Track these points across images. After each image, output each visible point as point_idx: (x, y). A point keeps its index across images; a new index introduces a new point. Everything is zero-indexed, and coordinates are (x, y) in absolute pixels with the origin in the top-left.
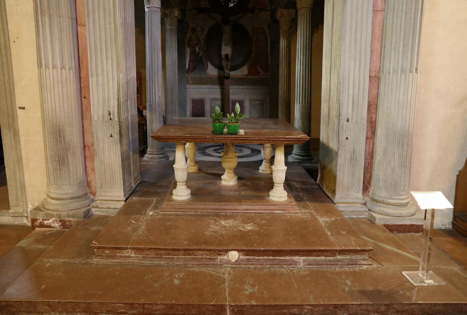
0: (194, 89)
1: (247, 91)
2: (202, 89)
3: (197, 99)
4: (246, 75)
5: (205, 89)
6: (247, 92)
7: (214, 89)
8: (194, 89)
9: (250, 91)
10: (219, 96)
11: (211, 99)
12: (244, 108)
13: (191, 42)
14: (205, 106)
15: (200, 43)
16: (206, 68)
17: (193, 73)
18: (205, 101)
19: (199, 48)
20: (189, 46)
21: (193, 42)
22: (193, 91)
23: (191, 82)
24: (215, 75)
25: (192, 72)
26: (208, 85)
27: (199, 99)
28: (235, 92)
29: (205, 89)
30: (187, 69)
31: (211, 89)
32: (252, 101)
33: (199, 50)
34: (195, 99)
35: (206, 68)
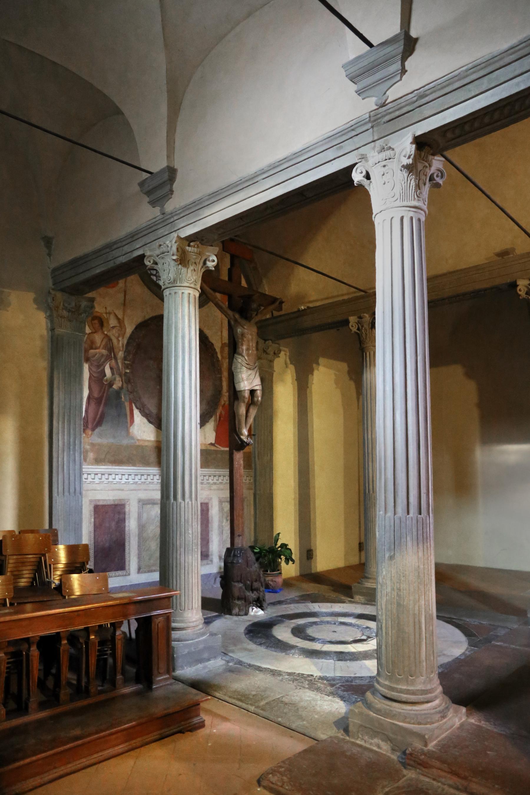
0: (99, 475)
1: (215, 481)
3: (109, 503)
5: (126, 476)
6: (215, 484)
8: (99, 475)
9: (220, 481)
10: (157, 495)
11: (140, 501)
12: (210, 521)
13: (92, 351)
14: (127, 524)
15: (114, 355)
16: (129, 421)
17: (97, 430)
18: (127, 510)
19: (111, 368)
20: (87, 360)
22: (97, 480)
23: (91, 455)
24: (148, 441)
25: (93, 430)
27: (112, 503)
29: (126, 476)
32: (223, 503)
33: (113, 374)
34: (101, 503)
35: (129, 421)
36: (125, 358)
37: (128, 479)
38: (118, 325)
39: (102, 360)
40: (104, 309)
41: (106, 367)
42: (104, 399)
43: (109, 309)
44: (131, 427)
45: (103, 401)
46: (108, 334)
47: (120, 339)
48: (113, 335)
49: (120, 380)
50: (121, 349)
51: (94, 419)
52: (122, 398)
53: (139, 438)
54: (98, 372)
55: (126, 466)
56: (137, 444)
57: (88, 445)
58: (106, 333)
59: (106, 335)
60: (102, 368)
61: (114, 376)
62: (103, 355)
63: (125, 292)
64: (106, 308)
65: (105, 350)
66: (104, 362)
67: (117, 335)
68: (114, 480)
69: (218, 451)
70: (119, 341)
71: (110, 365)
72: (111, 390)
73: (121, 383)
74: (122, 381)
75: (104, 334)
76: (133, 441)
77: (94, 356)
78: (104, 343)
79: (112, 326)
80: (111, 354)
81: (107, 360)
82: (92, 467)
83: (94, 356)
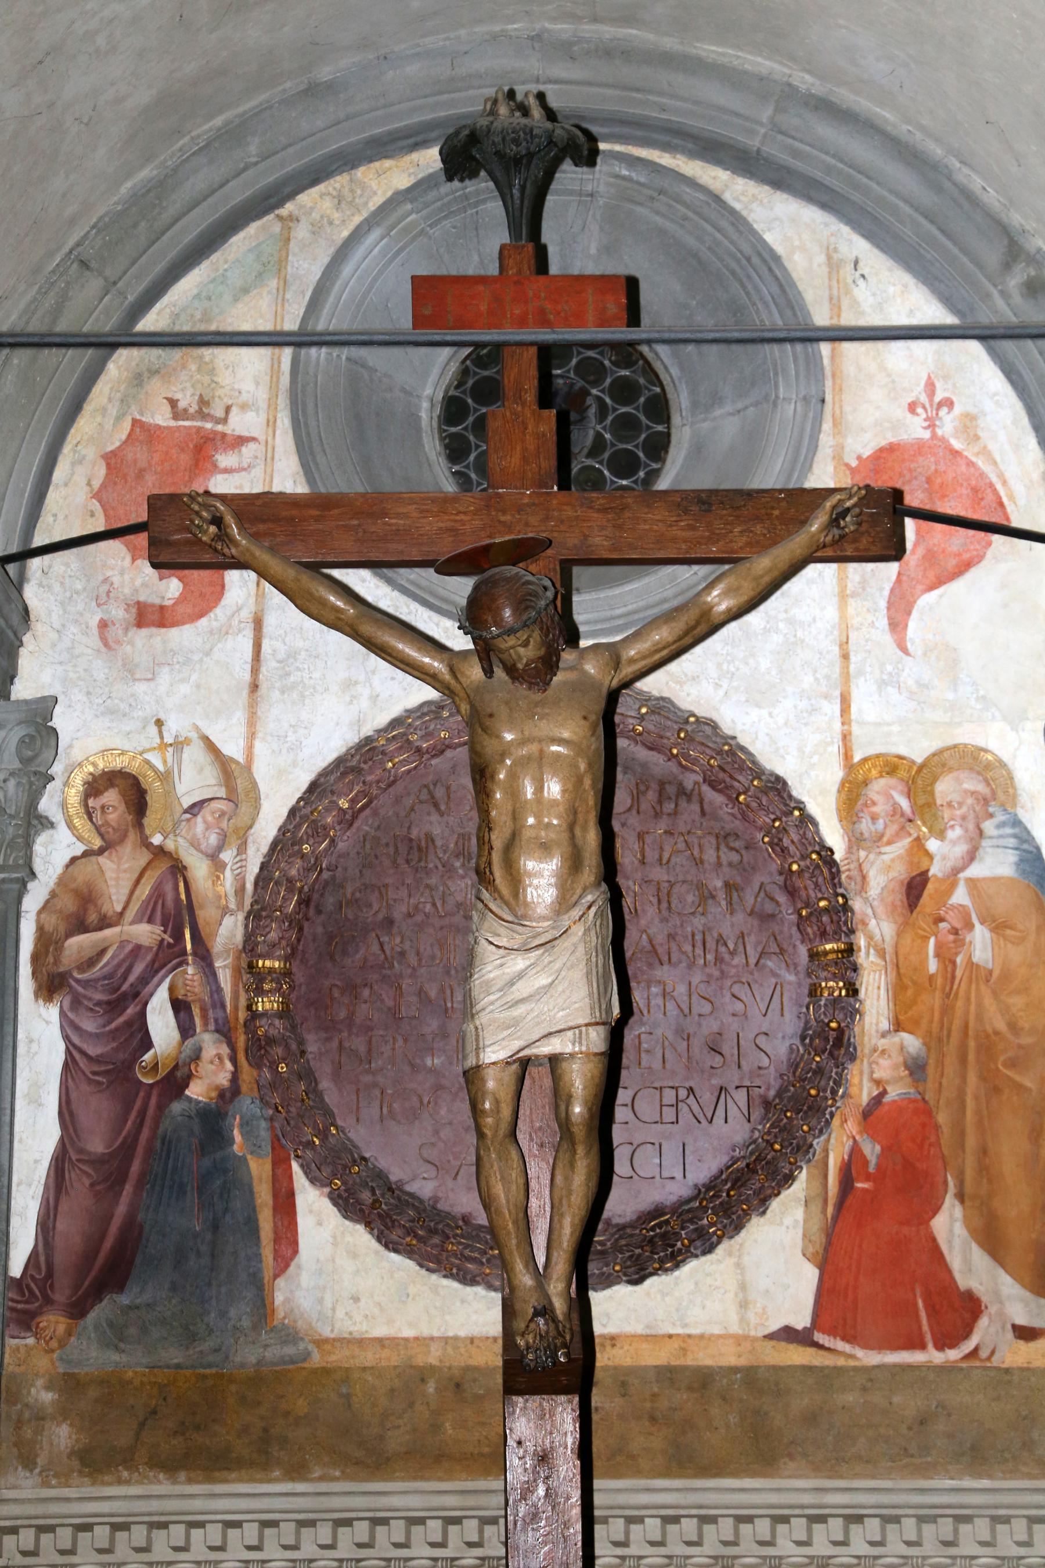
2: (214, 1535)
4: (788, 1334)
5: (251, 1533)
7: (376, 1522)
17: (100, 1312)
19: (179, 1006)
21: (107, 932)
25: (78, 1310)
26: (297, 1471)
28: (654, 1557)
30: (16, 1270)
31: (324, 1533)
33: (186, 1030)
36: (250, 947)
37: (258, 1548)
38: (222, 793)
39: (139, 969)
40: (153, 730)
41: (149, 1007)
42: (140, 1150)
43: (174, 727)
44: (280, 1282)
45: (135, 1167)
46: (170, 845)
47: (227, 856)
48: (195, 844)
49: (225, 1050)
50: (232, 905)
51: (89, 1256)
52: (231, 1141)
53: (326, 1332)
54: (114, 1034)
55: (252, 1480)
56: (316, 1359)
57: (48, 1388)
58: (157, 840)
59: (160, 852)
60: (131, 1011)
61: (190, 1042)
62: (137, 950)
63: (258, 623)
64: (159, 723)
65: (150, 921)
66: (144, 980)
67: (213, 839)
68: (182, 1556)
69: (839, 1371)
70: (218, 866)
71: (171, 990)
72: (177, 1107)
73: (229, 1066)
74: (234, 1060)
75: (148, 846)
76: (289, 1350)
77: (91, 962)
78: (145, 890)
79: (186, 803)
80: (179, 937)
81: (157, 971)
82: (66, 1492)
83: (91, 962)
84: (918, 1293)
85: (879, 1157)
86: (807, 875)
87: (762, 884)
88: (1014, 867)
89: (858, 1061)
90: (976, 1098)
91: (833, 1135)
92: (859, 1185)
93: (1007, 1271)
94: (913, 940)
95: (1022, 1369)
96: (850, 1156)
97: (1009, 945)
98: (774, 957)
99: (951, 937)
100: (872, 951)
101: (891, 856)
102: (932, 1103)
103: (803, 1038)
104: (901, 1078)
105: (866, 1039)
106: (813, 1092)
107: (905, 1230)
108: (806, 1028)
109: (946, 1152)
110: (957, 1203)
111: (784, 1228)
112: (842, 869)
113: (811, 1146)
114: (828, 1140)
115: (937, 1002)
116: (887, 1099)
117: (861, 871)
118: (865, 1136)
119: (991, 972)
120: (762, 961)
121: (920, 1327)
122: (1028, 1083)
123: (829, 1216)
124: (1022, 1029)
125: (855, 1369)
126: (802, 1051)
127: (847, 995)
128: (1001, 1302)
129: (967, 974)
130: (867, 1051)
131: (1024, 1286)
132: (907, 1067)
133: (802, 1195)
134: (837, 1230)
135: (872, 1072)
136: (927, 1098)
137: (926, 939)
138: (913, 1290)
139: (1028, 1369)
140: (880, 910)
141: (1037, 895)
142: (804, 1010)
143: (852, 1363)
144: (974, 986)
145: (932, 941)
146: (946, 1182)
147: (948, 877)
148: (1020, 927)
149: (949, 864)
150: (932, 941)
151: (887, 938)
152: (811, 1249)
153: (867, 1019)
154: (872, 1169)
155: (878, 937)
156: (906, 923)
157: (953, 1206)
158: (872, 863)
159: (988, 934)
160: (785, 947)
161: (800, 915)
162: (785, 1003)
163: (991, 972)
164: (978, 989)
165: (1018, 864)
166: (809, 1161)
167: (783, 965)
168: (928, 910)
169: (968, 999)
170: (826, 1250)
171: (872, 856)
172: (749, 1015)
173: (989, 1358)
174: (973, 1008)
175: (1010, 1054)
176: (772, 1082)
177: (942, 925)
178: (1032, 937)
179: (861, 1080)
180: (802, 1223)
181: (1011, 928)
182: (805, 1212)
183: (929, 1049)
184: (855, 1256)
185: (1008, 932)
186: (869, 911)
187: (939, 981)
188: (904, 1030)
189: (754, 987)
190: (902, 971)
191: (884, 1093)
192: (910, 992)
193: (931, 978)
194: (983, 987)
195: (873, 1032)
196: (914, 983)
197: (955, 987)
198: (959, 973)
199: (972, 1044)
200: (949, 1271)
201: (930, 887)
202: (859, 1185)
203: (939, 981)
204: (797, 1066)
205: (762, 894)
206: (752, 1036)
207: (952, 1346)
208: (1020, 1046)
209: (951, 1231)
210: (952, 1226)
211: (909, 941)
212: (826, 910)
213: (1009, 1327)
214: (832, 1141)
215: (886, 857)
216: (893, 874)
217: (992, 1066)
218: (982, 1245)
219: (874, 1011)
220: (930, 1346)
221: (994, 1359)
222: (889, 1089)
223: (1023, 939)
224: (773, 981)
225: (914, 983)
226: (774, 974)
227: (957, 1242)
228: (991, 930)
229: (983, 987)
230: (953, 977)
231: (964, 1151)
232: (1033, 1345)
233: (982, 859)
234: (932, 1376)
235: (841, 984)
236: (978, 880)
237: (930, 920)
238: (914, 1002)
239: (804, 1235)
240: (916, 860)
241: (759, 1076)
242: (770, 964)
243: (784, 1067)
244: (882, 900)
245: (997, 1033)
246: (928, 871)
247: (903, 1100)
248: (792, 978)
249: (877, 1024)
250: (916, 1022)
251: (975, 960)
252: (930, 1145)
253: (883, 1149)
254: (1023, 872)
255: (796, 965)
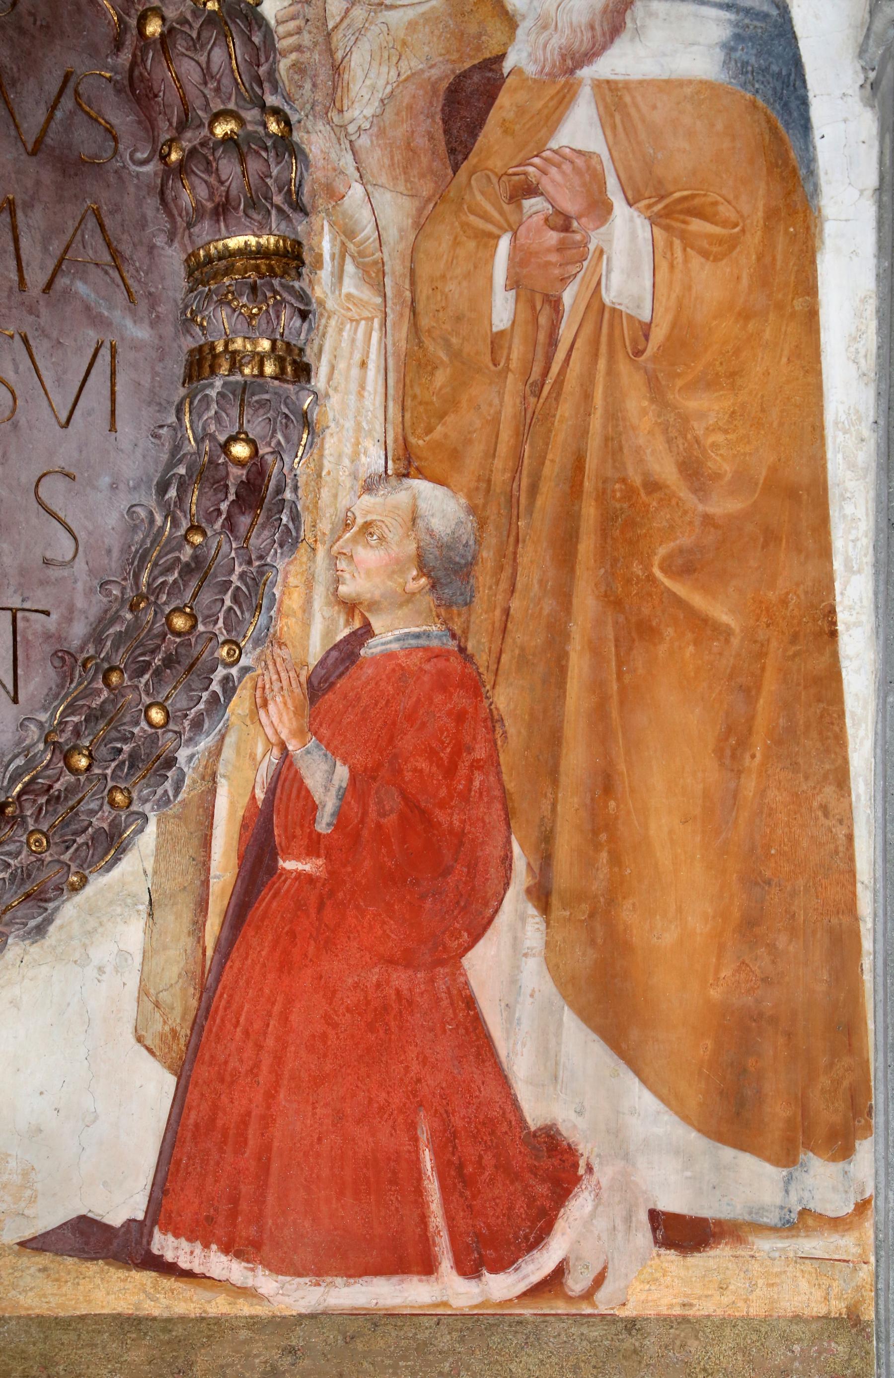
84: (424, 1136)
85: (342, 797)
86: (181, 46)
87: (67, 77)
88: (719, 55)
89: (303, 549)
90: (595, 650)
91: (231, 740)
92: (289, 865)
93: (644, 1081)
94: (456, 243)
95: (667, 1321)
96: (271, 792)
97: (696, 261)
98: (95, 274)
99: (553, 237)
100: (350, 267)
101: (410, 14)
102: (482, 659)
103: (162, 488)
104: (410, 598)
105: (325, 494)
106: (180, 622)
107: (400, 978)
108: (172, 464)
109: (511, 785)
110: (531, 910)
111: (91, 971)
112: (281, 45)
113: (171, 762)
114: (217, 751)
115: (509, 409)
116: (372, 649)
117: (331, 52)
118: (312, 742)
119: (646, 330)
120: (62, 282)
121: (423, 1220)
122: (723, 616)
123: (210, 941)
124: (716, 476)
125: (254, 1323)
126: (159, 519)
127: (280, 376)
128: (626, 1157)
129: (588, 329)
130: (325, 526)
131: (686, 1118)
132: (423, 568)
133: (141, 888)
134: (228, 977)
135: (338, 581)
136: (470, 646)
137: (489, 240)
138: (412, 1126)
139: (684, 1320)
140: (375, 158)
141: (773, 130)
142: (172, 419)
143: (245, 1308)
144: (602, 364)
145: (504, 244)
146: (507, 859)
147: (552, 76)
148: (725, 211)
149: (557, 41)
150: (504, 244)
151: (391, 235)
152: (157, 1026)
153: (330, 444)
154: (323, 824)
155: (368, 231)
156: (441, 197)
157: (523, 918)
158: (360, 32)
159: (643, 229)
160: (126, 248)
161: (164, 158)
162: (120, 398)
163: (646, 330)
164: (611, 372)
165: (729, 49)
166: (165, 801)
167: (121, 296)
168: (497, 163)
169: (587, 396)
170: (198, 1027)
171: (359, 13)
172: (22, 418)
173: (588, 1295)
174: (596, 423)
175: (685, 540)
176: (80, 603)
177: (532, 204)
178: (753, 240)
179: (308, 601)
180: (138, 959)
181: (699, 214)
182: (149, 931)
183: (482, 524)
184: (270, 1042)
185: (696, 225)
186: (347, 162)
187: (517, 351)
188: (421, 474)
189: (40, 347)
190: (425, 322)
191: (366, 632)
192: (441, 378)
193: (497, 341)
194: (623, 367)
195: (344, 477)
196: (456, 355)
197: (555, 369)
198: (566, 332)
199: (590, 512)
200: (503, 1080)
201: (504, 99)
202: (289, 865)
203: (517, 351)
204: (144, 558)
205: (67, 103)
206: (28, 477)
207: (499, 1266)
208: (708, 520)
209: (514, 981)
210: (516, 968)
211: (446, 241)
212: (228, 139)
213: (644, 1217)
214: (228, 752)
215: (392, 17)
216: (412, 64)
217: (637, 569)
218: (585, 1015)
219: (349, 424)
220: (446, 1264)
221: (601, 1296)
222: (376, 624)
223: (732, 244)
224: (92, 335)
225: (456, 355)
226: (97, 320)
227: (526, 1009)
228: (653, 221)
229: (623, 367)
230: (553, 342)
231: (555, 782)
232: (698, 1261)
233: (637, 32)
234: (444, 1341)
235: (265, 345)
236: (627, 85)
237: (502, 190)
238: (451, 404)
239: (143, 991)
240: (473, 29)
241: (42, 583)
242: (81, 288)
243: (114, 562)
244: (382, 132)
245: (653, 486)
246: (501, 57)
247: (411, 651)
248: (140, 332)
249: (355, 457)
250: (455, 456)
251: (609, 297)
252: (476, 765)
253: (353, 778)
254: (743, 68)
255: (153, 300)
